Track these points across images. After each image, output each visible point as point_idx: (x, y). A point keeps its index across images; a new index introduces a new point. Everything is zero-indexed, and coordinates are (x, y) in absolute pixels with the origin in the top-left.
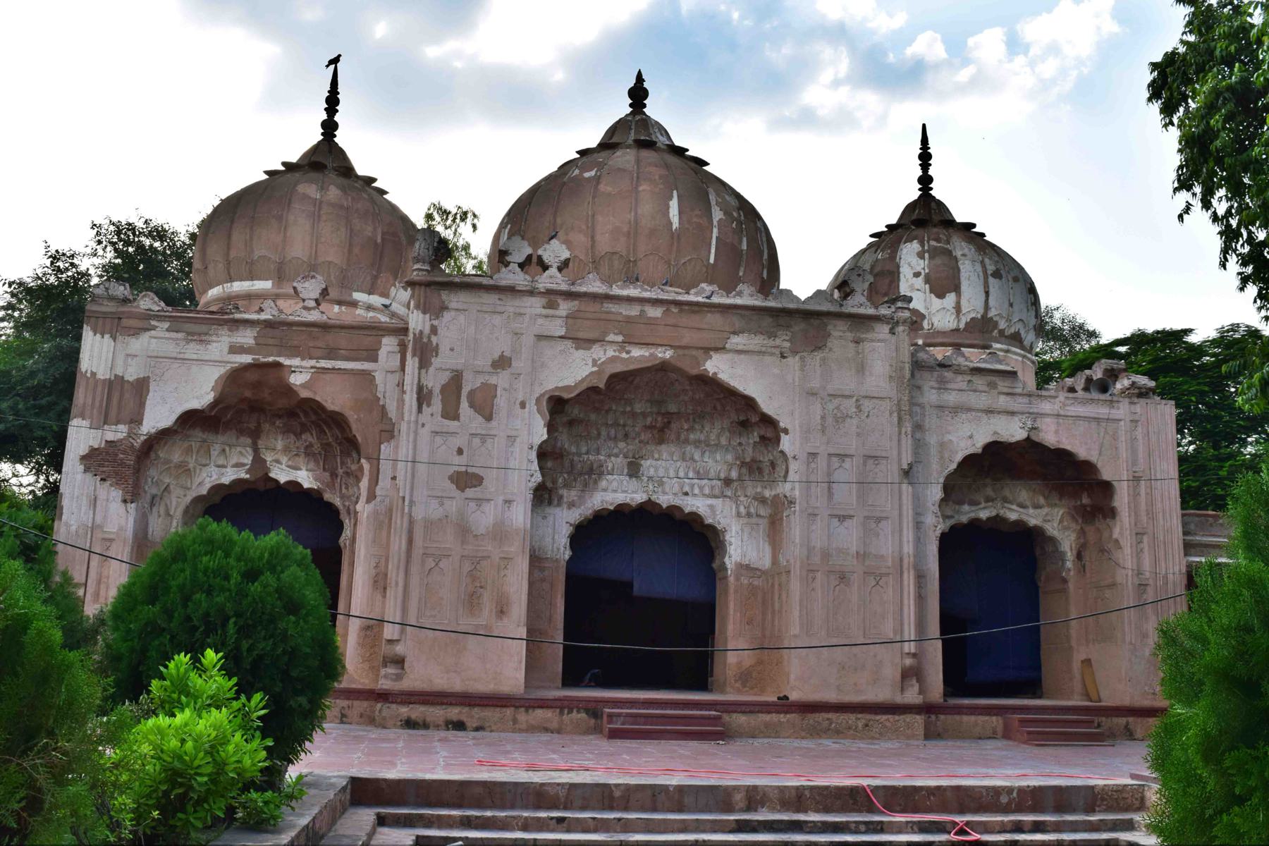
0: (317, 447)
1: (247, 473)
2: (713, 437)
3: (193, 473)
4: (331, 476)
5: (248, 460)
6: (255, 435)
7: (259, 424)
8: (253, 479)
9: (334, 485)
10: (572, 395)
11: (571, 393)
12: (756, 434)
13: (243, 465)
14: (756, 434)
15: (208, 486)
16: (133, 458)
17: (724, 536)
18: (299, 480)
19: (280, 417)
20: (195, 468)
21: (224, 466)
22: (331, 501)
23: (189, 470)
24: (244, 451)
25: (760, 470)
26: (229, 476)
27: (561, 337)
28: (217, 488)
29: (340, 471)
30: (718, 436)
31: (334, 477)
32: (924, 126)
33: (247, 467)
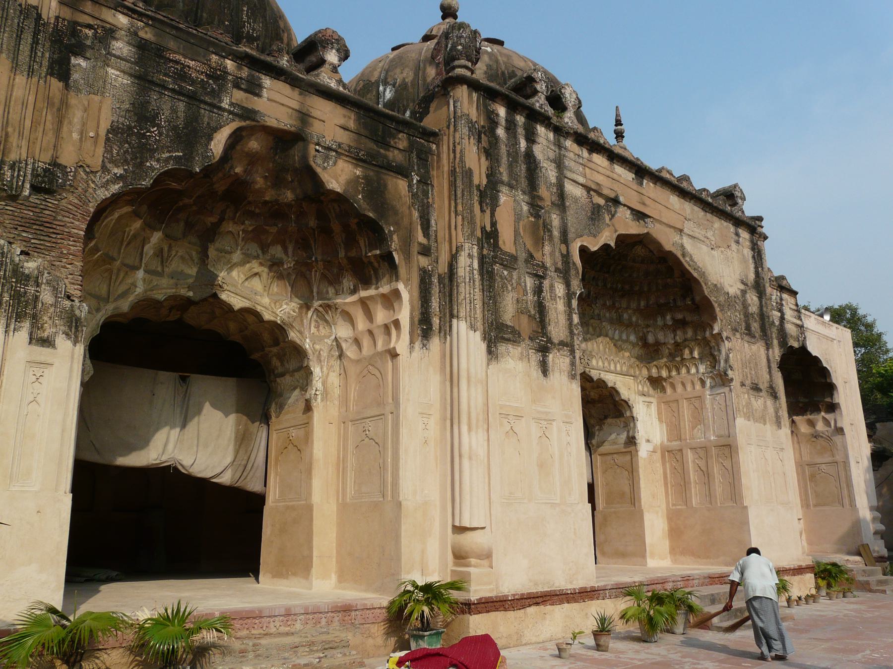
0: (289, 264)
1: (190, 288)
2: (625, 316)
3: (114, 277)
4: (301, 308)
5: (193, 271)
6: (208, 236)
7: (221, 220)
8: (197, 299)
9: (302, 321)
10: (596, 249)
11: (594, 246)
12: (668, 317)
13: (190, 276)
14: (668, 317)
15: (131, 298)
16: (84, 227)
17: (631, 412)
18: (259, 308)
19: (252, 215)
20: (119, 270)
21: (161, 274)
22: (298, 342)
23: (110, 271)
24: (187, 257)
25: (657, 351)
26: (164, 289)
27: (582, 185)
28: (147, 303)
29: (316, 304)
30: (630, 318)
31: (304, 310)
32: (617, 107)
33: (191, 281)
